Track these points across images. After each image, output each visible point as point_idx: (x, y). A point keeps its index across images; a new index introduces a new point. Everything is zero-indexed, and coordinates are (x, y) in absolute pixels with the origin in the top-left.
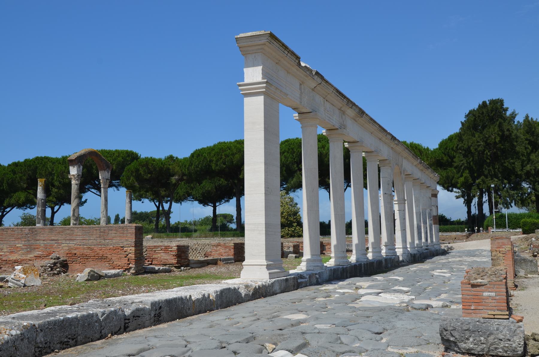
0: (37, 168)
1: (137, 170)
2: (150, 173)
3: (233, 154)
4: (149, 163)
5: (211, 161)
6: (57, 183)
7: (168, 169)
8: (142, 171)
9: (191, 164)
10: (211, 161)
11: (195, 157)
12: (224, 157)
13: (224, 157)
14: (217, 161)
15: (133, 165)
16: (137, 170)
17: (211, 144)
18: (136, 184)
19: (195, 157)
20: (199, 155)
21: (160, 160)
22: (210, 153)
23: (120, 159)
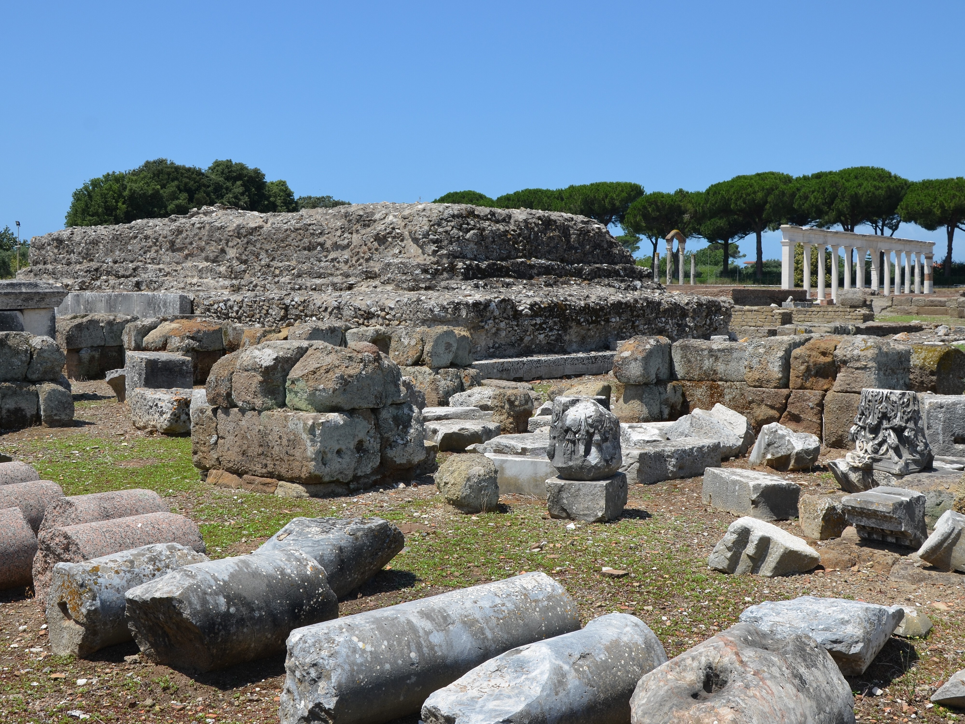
3: (755, 193)
4: (657, 199)
5: (730, 199)
7: (679, 206)
9: (707, 201)
10: (730, 199)
11: (711, 195)
12: (744, 196)
13: (744, 196)
14: (737, 200)
15: (638, 203)
16: (645, 207)
17: (729, 179)
19: (711, 195)
21: (669, 195)
22: (728, 191)
23: (624, 194)
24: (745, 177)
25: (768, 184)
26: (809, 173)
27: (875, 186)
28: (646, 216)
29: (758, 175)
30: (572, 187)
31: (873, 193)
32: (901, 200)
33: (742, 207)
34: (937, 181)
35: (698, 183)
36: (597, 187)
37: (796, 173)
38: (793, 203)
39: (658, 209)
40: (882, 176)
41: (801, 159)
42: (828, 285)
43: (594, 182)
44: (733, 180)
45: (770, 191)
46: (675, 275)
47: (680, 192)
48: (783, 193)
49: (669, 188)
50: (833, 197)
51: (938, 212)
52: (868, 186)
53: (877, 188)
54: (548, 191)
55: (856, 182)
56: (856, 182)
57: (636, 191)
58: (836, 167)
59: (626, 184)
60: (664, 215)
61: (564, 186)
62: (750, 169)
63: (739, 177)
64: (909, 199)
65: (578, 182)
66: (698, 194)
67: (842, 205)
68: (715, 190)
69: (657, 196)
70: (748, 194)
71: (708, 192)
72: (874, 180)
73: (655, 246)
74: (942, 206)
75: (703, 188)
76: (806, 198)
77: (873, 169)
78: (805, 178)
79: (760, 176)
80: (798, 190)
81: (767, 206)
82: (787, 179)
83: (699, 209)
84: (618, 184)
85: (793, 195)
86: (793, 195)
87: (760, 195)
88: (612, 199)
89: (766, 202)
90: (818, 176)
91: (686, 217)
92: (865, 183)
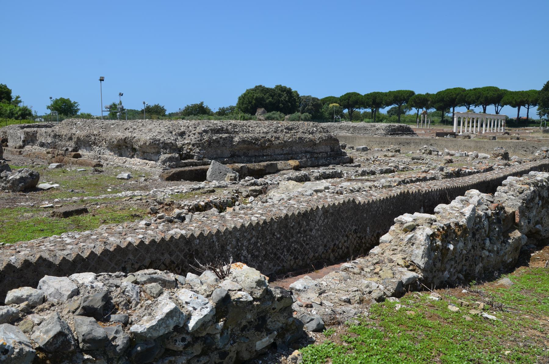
15: (413, 97)
17: (444, 90)
24: (449, 89)
25: (457, 92)
26: (472, 88)
28: (415, 102)
30: (390, 92)
32: (502, 98)
33: (447, 100)
34: (515, 92)
35: (433, 90)
36: (399, 92)
37: (467, 88)
39: (419, 100)
40: (496, 89)
41: (469, 83)
42: (477, 127)
44: (446, 90)
45: (458, 94)
46: (424, 122)
47: (427, 94)
48: (462, 95)
49: (424, 93)
50: (479, 97)
51: (514, 102)
53: (494, 94)
54: (382, 93)
55: (487, 92)
56: (487, 92)
57: (412, 93)
58: (481, 86)
59: (409, 91)
60: (422, 101)
61: (387, 91)
62: (452, 87)
63: (448, 89)
64: (505, 98)
65: (392, 90)
66: (433, 95)
67: (482, 100)
68: (439, 93)
69: (420, 95)
71: (437, 94)
73: (418, 111)
74: (516, 101)
75: (435, 93)
76: (470, 97)
77: (494, 87)
78: (471, 90)
82: (464, 90)
83: (433, 100)
84: (406, 91)
85: (466, 96)
86: (466, 96)
87: (454, 96)
90: (475, 89)
91: (429, 102)
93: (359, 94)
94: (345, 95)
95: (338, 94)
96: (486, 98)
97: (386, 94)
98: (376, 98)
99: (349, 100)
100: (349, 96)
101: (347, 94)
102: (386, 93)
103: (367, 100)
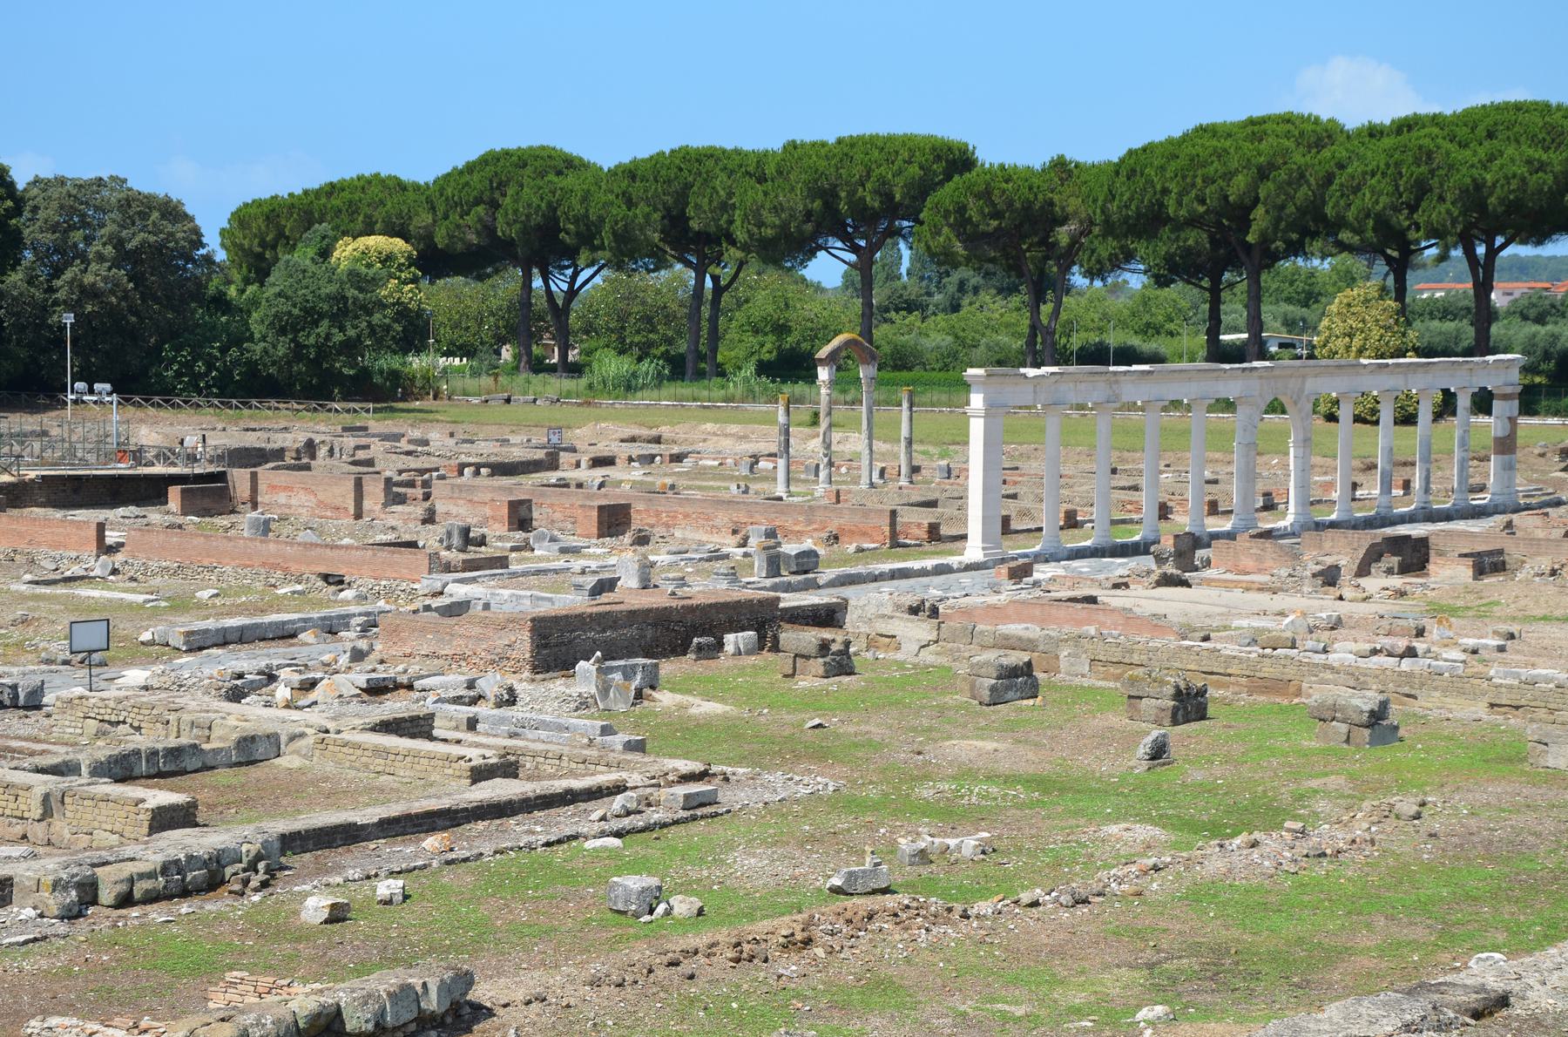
0: (688, 186)
1: (961, 209)
2: (997, 215)
6: (741, 235)
8: (973, 213)
9: (1112, 196)
18: (959, 248)
20: (1133, 171)
23: (914, 170)
27: (1529, 162)
29: (1252, 122)
31: (1523, 180)
36: (849, 147)
38: (1324, 203)
43: (845, 133)
50: (1422, 189)
52: (1514, 159)
62: (1231, 111)
63: (1201, 130)
68: (1134, 164)
70: (1209, 181)
72: (1534, 140)
79: (1256, 128)
80: (1341, 167)
81: (1259, 212)
87: (1241, 182)
88: (883, 181)
89: (1256, 200)
92: (1510, 151)
93: (570, 164)
94: (470, 168)
95: (425, 159)
96: (1474, 196)
97: (755, 168)
98: (682, 196)
99: (494, 205)
100: (496, 174)
101: (489, 160)
102: (762, 157)
103: (619, 211)
